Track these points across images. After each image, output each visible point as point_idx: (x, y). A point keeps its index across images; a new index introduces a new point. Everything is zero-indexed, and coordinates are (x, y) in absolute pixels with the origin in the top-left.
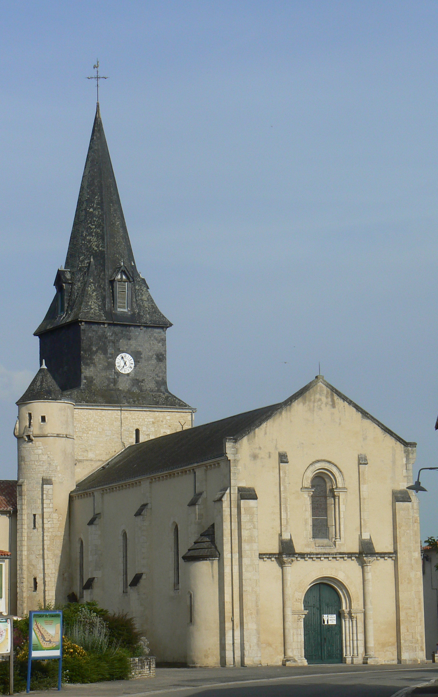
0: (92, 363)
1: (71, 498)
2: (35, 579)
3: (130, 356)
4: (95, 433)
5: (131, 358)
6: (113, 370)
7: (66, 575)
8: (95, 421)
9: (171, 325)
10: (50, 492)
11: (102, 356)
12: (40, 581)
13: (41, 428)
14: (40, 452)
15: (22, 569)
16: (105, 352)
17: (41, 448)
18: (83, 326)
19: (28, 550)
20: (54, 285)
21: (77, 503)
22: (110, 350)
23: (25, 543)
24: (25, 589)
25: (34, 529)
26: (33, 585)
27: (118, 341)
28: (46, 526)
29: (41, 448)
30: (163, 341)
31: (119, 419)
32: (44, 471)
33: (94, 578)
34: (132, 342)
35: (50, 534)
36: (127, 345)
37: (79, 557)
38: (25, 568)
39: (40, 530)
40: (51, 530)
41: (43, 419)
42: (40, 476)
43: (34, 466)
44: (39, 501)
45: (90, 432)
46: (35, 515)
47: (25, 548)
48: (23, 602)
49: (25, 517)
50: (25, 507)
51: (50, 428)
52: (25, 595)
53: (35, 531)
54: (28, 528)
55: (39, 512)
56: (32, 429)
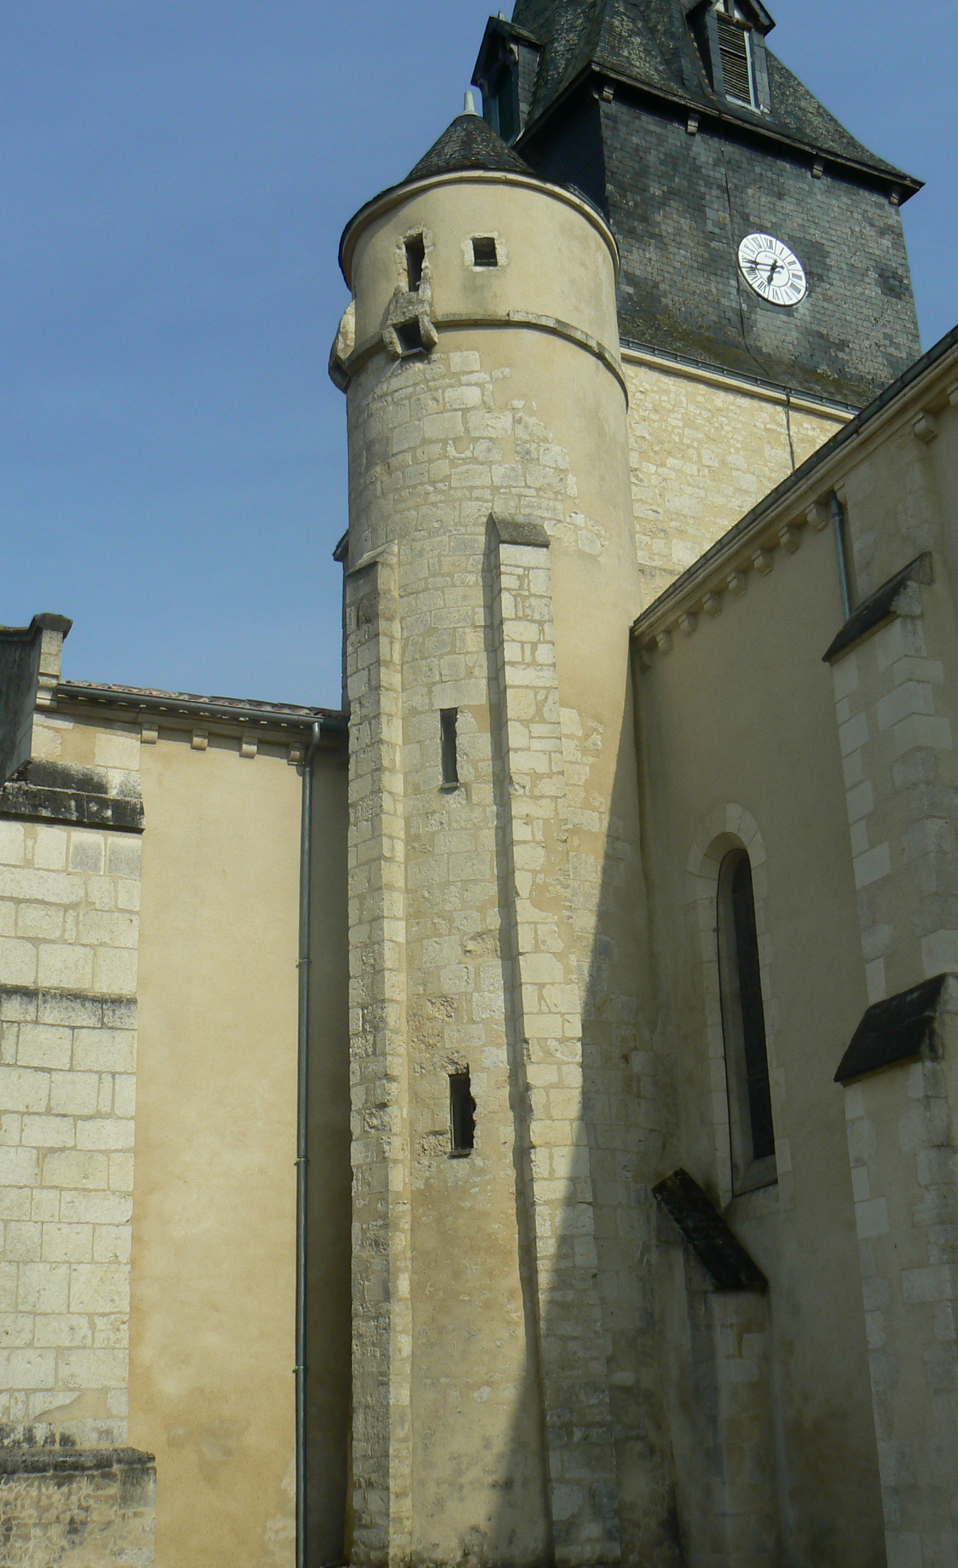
0: (652, 236)
1: (643, 647)
2: (460, 1084)
3: (787, 251)
4: (691, 469)
5: (793, 258)
6: (733, 282)
7: (639, 1062)
8: (688, 423)
9: (921, 184)
10: (538, 583)
11: (685, 223)
12: (489, 1093)
13: (472, 287)
14: (472, 396)
15: (376, 1025)
16: (697, 209)
17: (473, 378)
18: (609, 107)
19: (414, 915)
20: (474, 82)
21: (680, 663)
22: (717, 213)
23: (394, 874)
24: (398, 1147)
25: (446, 791)
26: (445, 1119)
27: (741, 189)
28: (517, 763)
29: (473, 378)
30: (896, 233)
31: (784, 439)
32: (495, 489)
33: (933, 988)
34: (788, 205)
35: (543, 810)
36: (774, 211)
37: (708, 946)
38: (395, 1016)
39: (484, 792)
40: (547, 787)
41: (485, 252)
42: (476, 512)
43: (443, 467)
44: (474, 641)
45: (670, 461)
46: (449, 718)
47: (395, 904)
48: (387, 1223)
49: (393, 731)
50: (391, 678)
51: (513, 291)
52: (399, 1179)
53: (453, 801)
54: (414, 790)
55: (474, 695)
56: (426, 291)
